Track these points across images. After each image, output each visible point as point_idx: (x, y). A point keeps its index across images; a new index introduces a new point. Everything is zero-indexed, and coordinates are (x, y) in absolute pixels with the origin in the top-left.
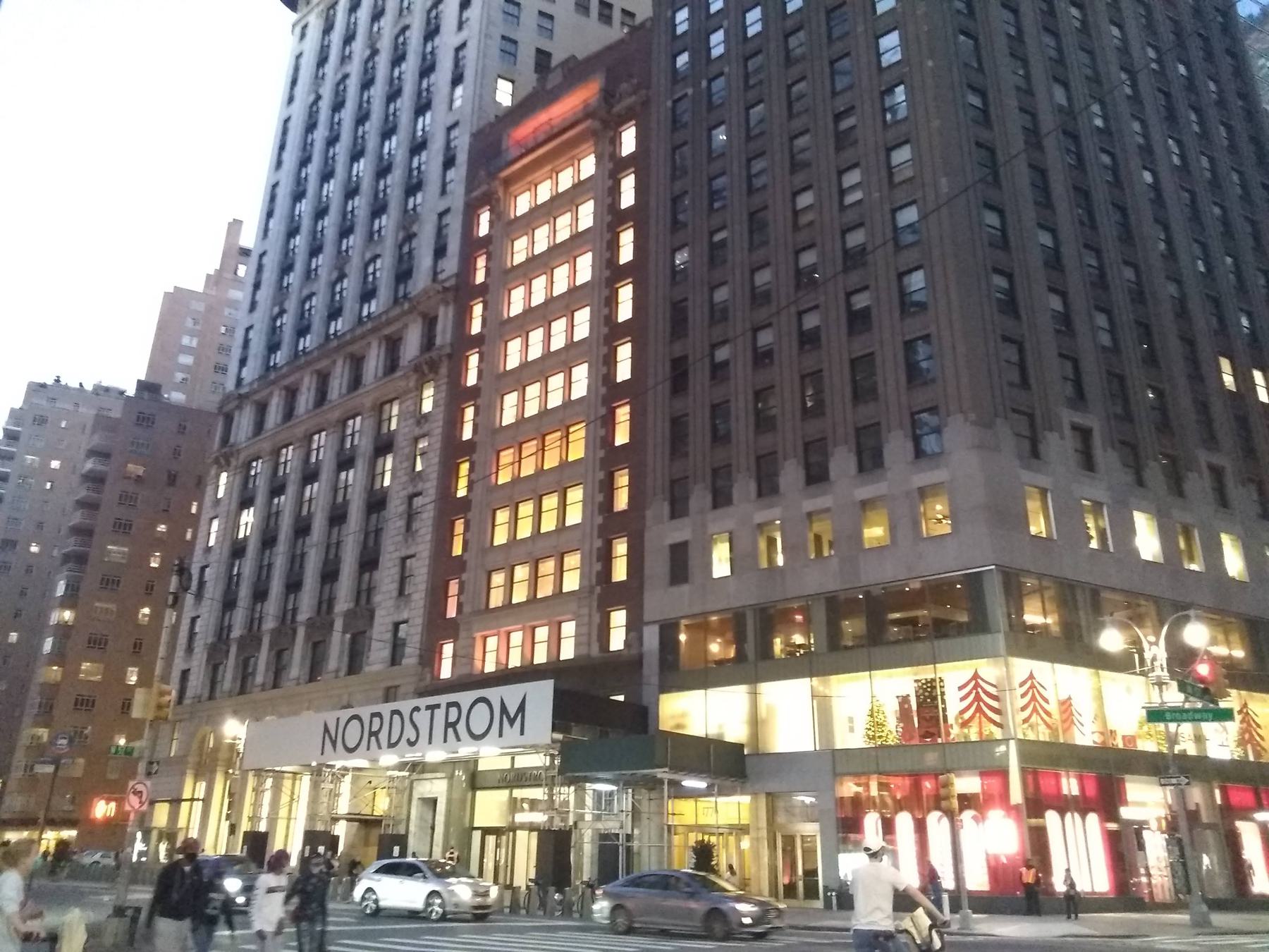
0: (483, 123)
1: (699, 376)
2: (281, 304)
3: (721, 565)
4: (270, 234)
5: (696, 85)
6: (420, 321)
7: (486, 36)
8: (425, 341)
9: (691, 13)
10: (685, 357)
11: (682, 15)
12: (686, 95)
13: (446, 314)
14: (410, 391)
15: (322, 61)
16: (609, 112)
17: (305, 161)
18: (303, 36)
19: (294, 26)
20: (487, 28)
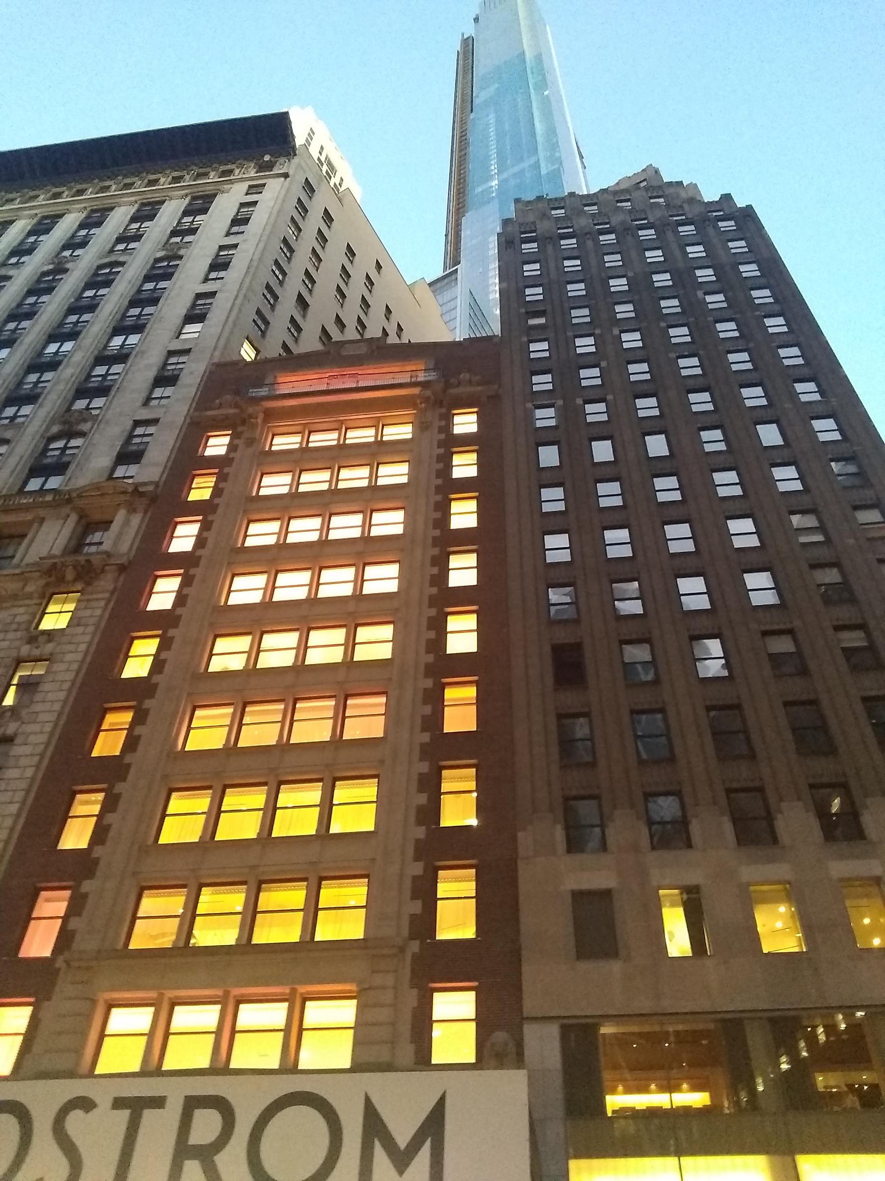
0: (223, 360)
3: (677, 940)
6: (73, 518)
7: (245, 296)
8: (74, 542)
10: (578, 647)
13: (127, 522)
14: (30, 596)
16: (444, 391)
20: (248, 290)
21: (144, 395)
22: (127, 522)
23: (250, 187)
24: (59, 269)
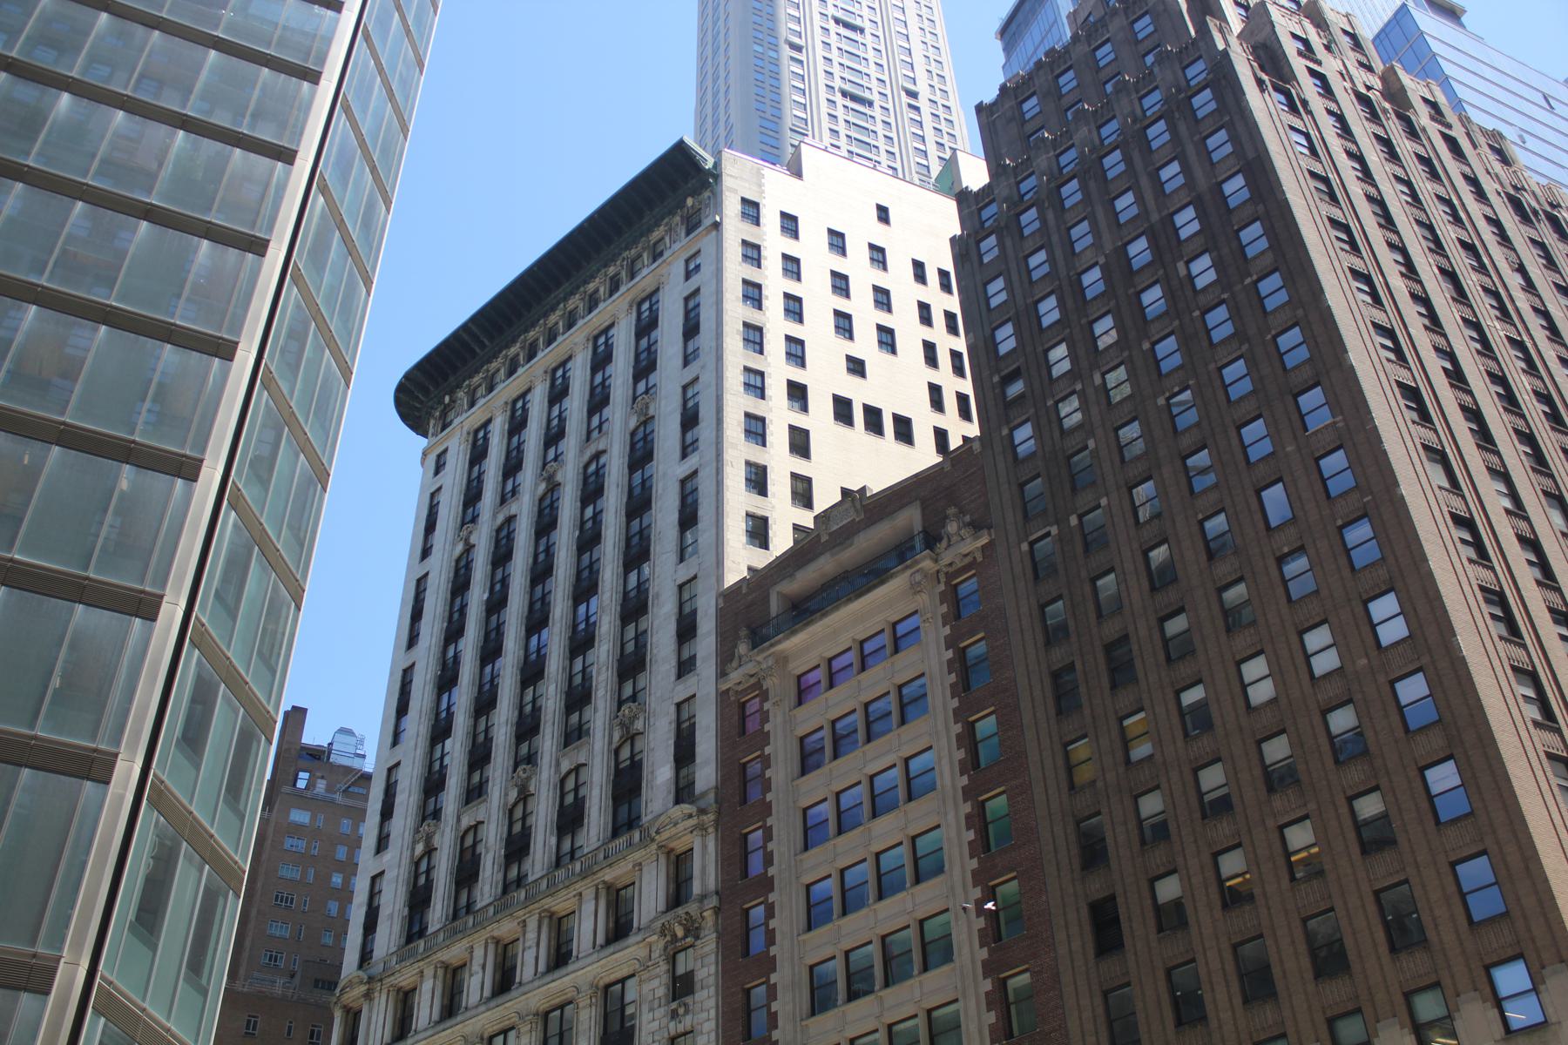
1: (1136, 926)
2: (429, 839)
4: (404, 737)
5: (1061, 521)
8: (672, 886)
9: (1038, 430)
11: (1024, 433)
12: (1048, 534)
13: (704, 847)
15: (472, 496)
17: (453, 633)
18: (439, 467)
19: (425, 454)
21: (674, 662)
22: (704, 847)
23: (687, 261)
24: (553, 487)
